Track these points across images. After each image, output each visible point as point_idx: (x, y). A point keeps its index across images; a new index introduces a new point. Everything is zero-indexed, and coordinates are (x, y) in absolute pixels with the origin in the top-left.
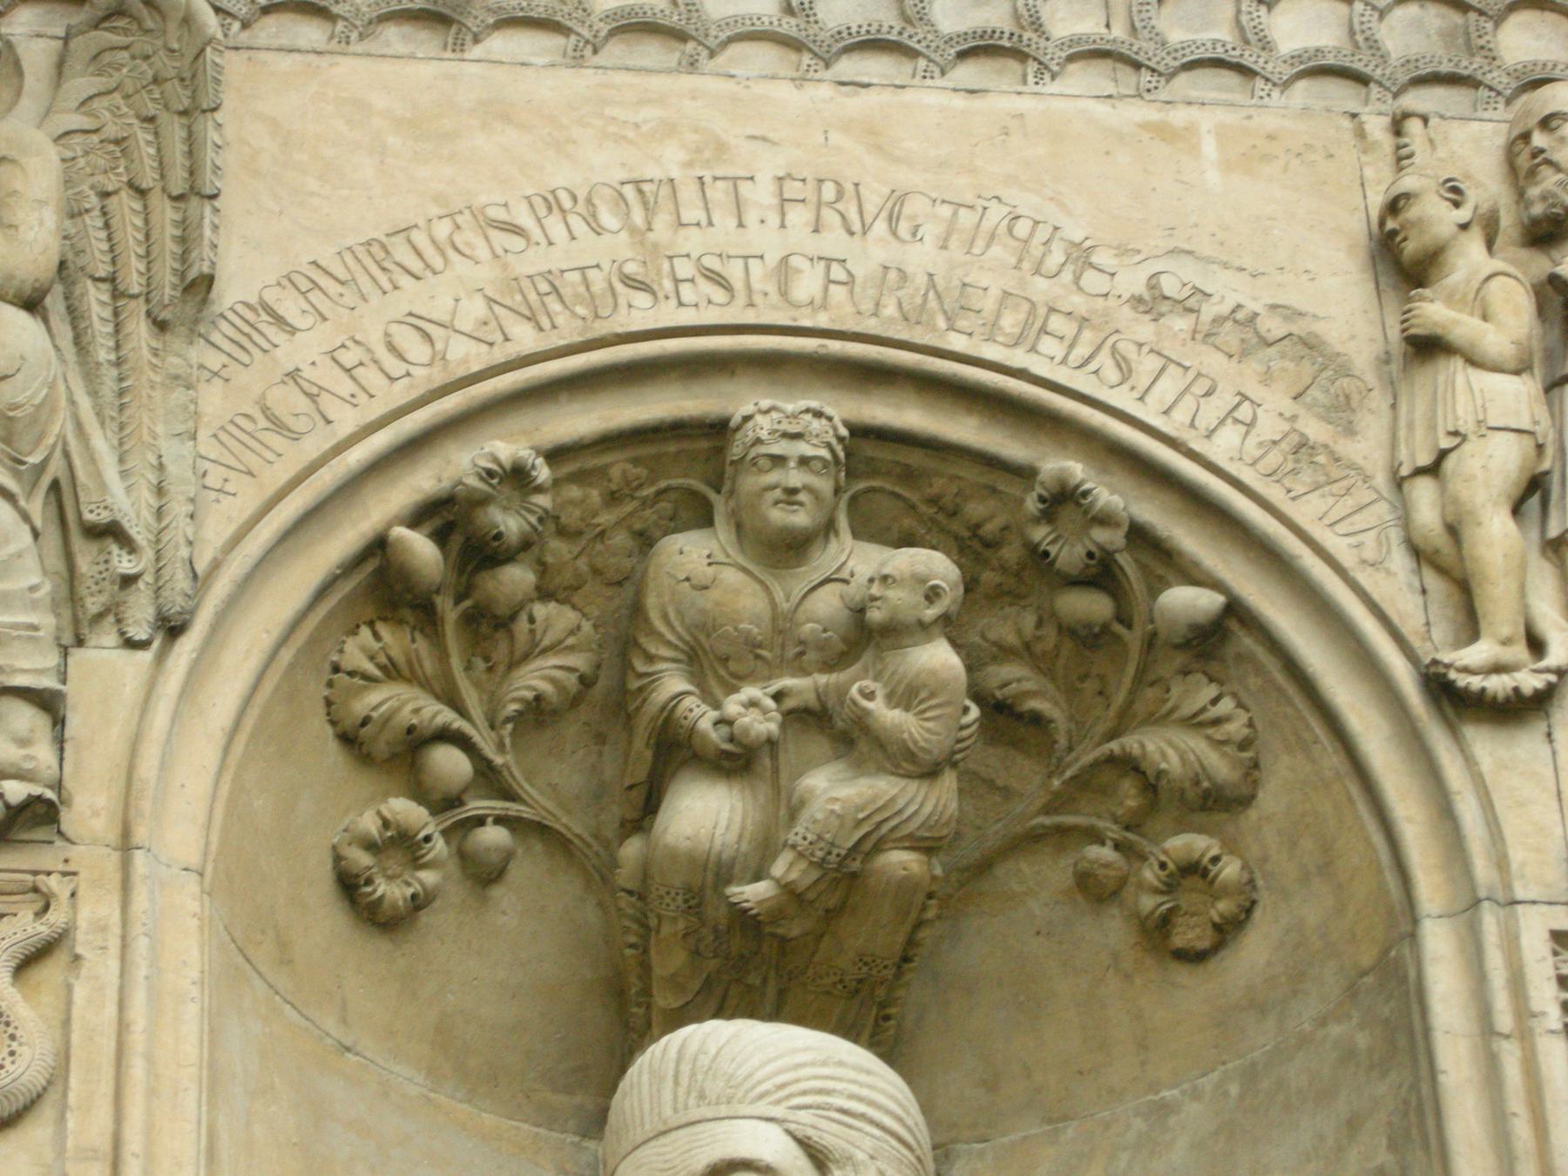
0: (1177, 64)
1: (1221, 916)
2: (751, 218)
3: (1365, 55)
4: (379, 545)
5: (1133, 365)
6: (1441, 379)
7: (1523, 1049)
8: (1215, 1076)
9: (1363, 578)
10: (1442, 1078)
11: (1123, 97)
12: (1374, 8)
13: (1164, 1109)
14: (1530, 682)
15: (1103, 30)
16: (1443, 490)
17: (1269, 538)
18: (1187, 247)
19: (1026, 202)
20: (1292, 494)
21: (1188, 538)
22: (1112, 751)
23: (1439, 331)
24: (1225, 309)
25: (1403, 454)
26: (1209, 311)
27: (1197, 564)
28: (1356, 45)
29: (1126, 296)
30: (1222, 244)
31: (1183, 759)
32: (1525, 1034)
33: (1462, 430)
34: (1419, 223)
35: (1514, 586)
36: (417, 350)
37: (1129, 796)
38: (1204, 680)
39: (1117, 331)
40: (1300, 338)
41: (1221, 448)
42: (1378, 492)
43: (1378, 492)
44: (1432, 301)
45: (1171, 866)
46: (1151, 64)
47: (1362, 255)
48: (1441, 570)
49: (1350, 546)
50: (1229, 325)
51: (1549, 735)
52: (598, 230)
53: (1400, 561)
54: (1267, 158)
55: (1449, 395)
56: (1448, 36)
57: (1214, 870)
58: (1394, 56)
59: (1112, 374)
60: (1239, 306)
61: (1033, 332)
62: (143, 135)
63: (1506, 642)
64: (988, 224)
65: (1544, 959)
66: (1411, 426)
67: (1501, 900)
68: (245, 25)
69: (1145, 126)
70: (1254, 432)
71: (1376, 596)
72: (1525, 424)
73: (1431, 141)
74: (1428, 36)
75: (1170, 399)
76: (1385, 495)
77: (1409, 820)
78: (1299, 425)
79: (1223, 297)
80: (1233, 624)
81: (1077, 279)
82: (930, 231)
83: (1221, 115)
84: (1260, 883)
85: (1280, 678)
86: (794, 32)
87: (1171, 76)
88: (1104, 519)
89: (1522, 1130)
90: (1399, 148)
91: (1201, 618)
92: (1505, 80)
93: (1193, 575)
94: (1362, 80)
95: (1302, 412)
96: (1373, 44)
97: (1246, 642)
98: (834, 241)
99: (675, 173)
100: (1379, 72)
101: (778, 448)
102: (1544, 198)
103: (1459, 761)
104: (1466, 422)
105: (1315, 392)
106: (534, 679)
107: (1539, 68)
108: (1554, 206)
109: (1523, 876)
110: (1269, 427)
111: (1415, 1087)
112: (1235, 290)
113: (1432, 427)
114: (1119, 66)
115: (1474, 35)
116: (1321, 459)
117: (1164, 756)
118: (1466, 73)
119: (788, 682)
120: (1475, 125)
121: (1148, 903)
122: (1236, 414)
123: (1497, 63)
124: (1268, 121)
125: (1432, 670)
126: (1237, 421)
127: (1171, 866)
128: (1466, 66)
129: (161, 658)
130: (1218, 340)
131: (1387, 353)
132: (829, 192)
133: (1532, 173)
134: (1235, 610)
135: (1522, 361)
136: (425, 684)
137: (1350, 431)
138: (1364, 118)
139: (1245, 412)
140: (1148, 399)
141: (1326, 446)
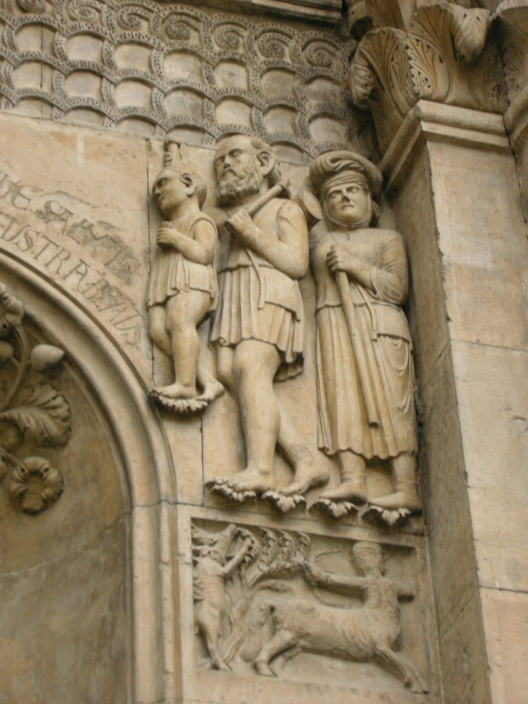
0: (70, 107)
1: (47, 496)
3: (156, 113)
5: (34, 242)
6: (171, 264)
7: (173, 570)
8: (36, 567)
9: (127, 350)
10: (135, 580)
11: (43, 119)
12: (162, 91)
13: (11, 581)
14: (195, 404)
15: (39, 87)
16: (167, 314)
17: (85, 326)
18: (64, 190)
20: (99, 309)
22: (5, 417)
23: (173, 242)
24: (79, 221)
25: (151, 296)
26: (71, 221)
27: (52, 336)
28: (152, 108)
29: (34, 210)
30: (81, 191)
31: (37, 424)
32: (174, 564)
33: (178, 288)
34: (170, 192)
35: (193, 361)
37: (11, 437)
38: (50, 388)
39: (29, 226)
40: (111, 238)
42: (137, 311)
43: (137, 311)
44: (172, 228)
45: (26, 471)
46: (59, 106)
47: (144, 203)
48: (162, 350)
49: (122, 334)
50: (79, 229)
51: (201, 429)
53: (144, 344)
54: (105, 154)
55: (174, 271)
56: (194, 108)
57: (45, 475)
58: (168, 114)
59: (24, 245)
60: (85, 220)
63: (187, 385)
65: (187, 530)
66: (156, 283)
67: (171, 501)
69: (53, 134)
70: (85, 279)
71: (131, 359)
72: (207, 288)
73: (180, 155)
74: (185, 107)
75: (49, 259)
76: (141, 313)
77: (135, 461)
78: (107, 278)
79: (78, 216)
80: (66, 365)
81: (13, 201)
83: (88, 133)
84: (66, 482)
85: (85, 391)
87: (67, 112)
88: (13, 311)
89: (168, 606)
90: (165, 156)
91: (52, 360)
92: (217, 131)
93: (50, 340)
94: (153, 124)
95: (108, 271)
96: (160, 108)
97: (71, 373)
100: (161, 121)
102: (227, 187)
103: (160, 436)
104: (180, 285)
105: (115, 264)
107: (233, 128)
108: (231, 191)
109: (182, 492)
110: (92, 277)
111: (123, 582)
112: (84, 213)
113: (165, 285)
114: (44, 105)
115: (205, 109)
116: (114, 294)
117: (28, 421)
118: (199, 126)
120: (201, 150)
121: (14, 486)
122: (78, 270)
123: (215, 123)
124: (109, 138)
125: (152, 395)
126: (78, 272)
127: (26, 471)
128: (200, 123)
130: (74, 235)
131: (149, 249)
133: (224, 175)
135: (208, 259)
137: (129, 282)
138: (152, 141)
139: (82, 269)
140: (39, 258)
141: (117, 288)
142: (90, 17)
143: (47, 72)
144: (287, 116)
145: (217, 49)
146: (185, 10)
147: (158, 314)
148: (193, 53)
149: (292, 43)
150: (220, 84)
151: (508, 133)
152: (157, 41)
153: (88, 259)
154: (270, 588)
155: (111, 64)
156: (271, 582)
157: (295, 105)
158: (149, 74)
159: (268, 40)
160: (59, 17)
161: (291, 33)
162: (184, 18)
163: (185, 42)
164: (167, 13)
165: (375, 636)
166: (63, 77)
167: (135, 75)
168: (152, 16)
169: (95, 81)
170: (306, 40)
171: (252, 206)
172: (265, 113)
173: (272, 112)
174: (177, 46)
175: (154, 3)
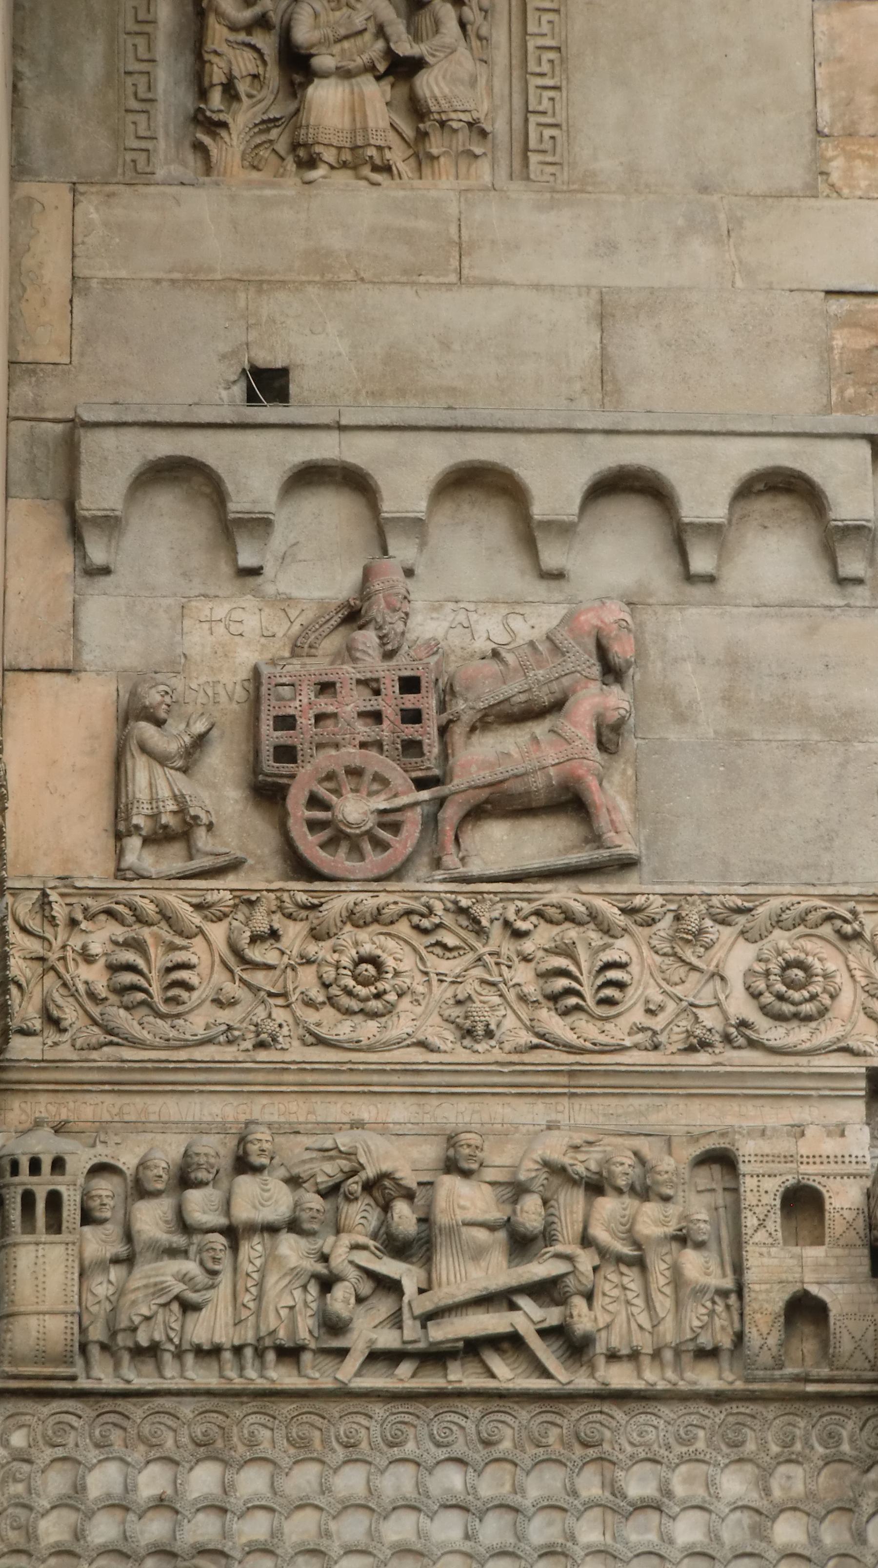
3: (714, 1545)
68: (240, 1562)
86: (469, 1551)
96: (718, 1538)
128: (759, 1546)
142: (647, 1438)
143: (609, 1516)
144: (845, 1518)
145: (775, 1449)
146: (742, 1410)
148: (750, 1461)
149: (850, 1425)
150: (777, 1493)
152: (714, 1454)
155: (668, 1493)
157: (852, 1505)
158: (708, 1498)
159: (825, 1428)
160: (617, 1447)
161: (848, 1414)
162: (740, 1419)
163: (741, 1449)
164: (722, 1416)
166: (623, 1520)
167: (694, 1503)
168: (709, 1422)
169: (654, 1516)
170: (864, 1418)
172: (822, 1520)
173: (830, 1517)
174: (734, 1457)
175: (709, 1407)
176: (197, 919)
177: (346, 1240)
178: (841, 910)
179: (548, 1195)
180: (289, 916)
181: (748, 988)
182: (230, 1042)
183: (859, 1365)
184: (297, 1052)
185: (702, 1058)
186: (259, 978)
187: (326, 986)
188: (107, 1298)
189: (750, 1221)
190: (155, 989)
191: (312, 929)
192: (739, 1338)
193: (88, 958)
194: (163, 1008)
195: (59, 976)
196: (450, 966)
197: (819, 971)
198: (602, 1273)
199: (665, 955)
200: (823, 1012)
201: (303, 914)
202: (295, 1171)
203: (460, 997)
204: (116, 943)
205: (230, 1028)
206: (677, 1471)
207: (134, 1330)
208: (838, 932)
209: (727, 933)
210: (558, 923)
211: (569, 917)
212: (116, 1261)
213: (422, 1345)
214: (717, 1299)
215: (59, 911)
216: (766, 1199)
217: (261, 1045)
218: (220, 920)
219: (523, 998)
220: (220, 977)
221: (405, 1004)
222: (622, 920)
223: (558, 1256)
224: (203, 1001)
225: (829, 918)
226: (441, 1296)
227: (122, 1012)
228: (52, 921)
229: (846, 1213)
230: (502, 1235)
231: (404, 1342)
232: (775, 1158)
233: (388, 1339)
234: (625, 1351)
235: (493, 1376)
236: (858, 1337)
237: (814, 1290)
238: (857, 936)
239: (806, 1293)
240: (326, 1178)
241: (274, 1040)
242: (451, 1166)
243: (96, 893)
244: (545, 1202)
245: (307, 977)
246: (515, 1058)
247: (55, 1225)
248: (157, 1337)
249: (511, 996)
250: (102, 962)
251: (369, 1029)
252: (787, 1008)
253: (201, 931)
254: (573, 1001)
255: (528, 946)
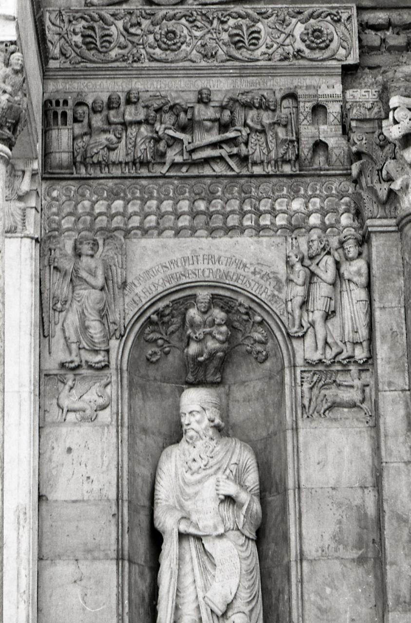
2: (199, 263)
4: (149, 317)
14: (300, 334)
19: (238, 256)
21: (258, 310)
36: (153, 289)
41: (263, 297)
52: (178, 266)
53: (285, 314)
59: (248, 285)
61: (237, 280)
62: (116, 257)
64: (233, 260)
82: (224, 263)
98: (211, 266)
99: (189, 255)
101: (202, 301)
106: (171, 329)
110: (269, 293)
119: (205, 330)
129: (121, 340)
132: (210, 257)
134: (263, 320)
136: (157, 332)
147: (289, 304)
151: (398, 225)
153: (268, 287)
154: (325, 389)
156: (325, 387)
165: (356, 401)
171: (317, 261)
176: (112, 19)
177: (163, 126)
178: (334, 12)
179: (233, 110)
180: (144, 18)
181: (301, 39)
182: (124, 61)
183: (338, 164)
184: (147, 64)
185: (286, 63)
186: (135, 39)
187: (156, 41)
188: (83, 147)
189: (302, 117)
190: (98, 43)
191: (152, 22)
192: (298, 157)
193: (75, 33)
194: (101, 50)
195: (65, 39)
196: (198, 34)
197: (326, 32)
198: (250, 136)
199: (273, 28)
200: (327, 46)
201: (149, 17)
202: (147, 103)
203: (203, 44)
204: (84, 28)
205: (124, 56)
206: (277, 201)
207: (92, 157)
208: (332, 19)
209: (294, 21)
210: (236, 18)
211: (240, 16)
212: (85, 134)
213: (190, 161)
214: (290, 144)
215: (66, 19)
216: (307, 110)
217: (134, 61)
218: (120, 20)
219: (224, 44)
220: (122, 39)
221: (184, 47)
222: (258, 17)
223: (237, 130)
224: (115, 47)
225: (329, 14)
226: (197, 143)
227: (87, 51)
228: (63, 21)
229: (334, 114)
230: (217, 124)
231: (184, 160)
232: (310, 96)
233: (179, 159)
234: (259, 161)
235: (214, 171)
236: (338, 155)
237: (323, 139)
238: (339, 20)
239: (320, 140)
240: (157, 106)
241: (139, 60)
242: (200, 101)
243: (77, 11)
244: (232, 113)
245: (151, 38)
246: (221, 64)
247: (65, 123)
248: (100, 159)
249: (220, 43)
250: (80, 35)
251: (171, 56)
252: (314, 45)
253: (113, 23)
254: (241, 44)
255: (226, 27)
